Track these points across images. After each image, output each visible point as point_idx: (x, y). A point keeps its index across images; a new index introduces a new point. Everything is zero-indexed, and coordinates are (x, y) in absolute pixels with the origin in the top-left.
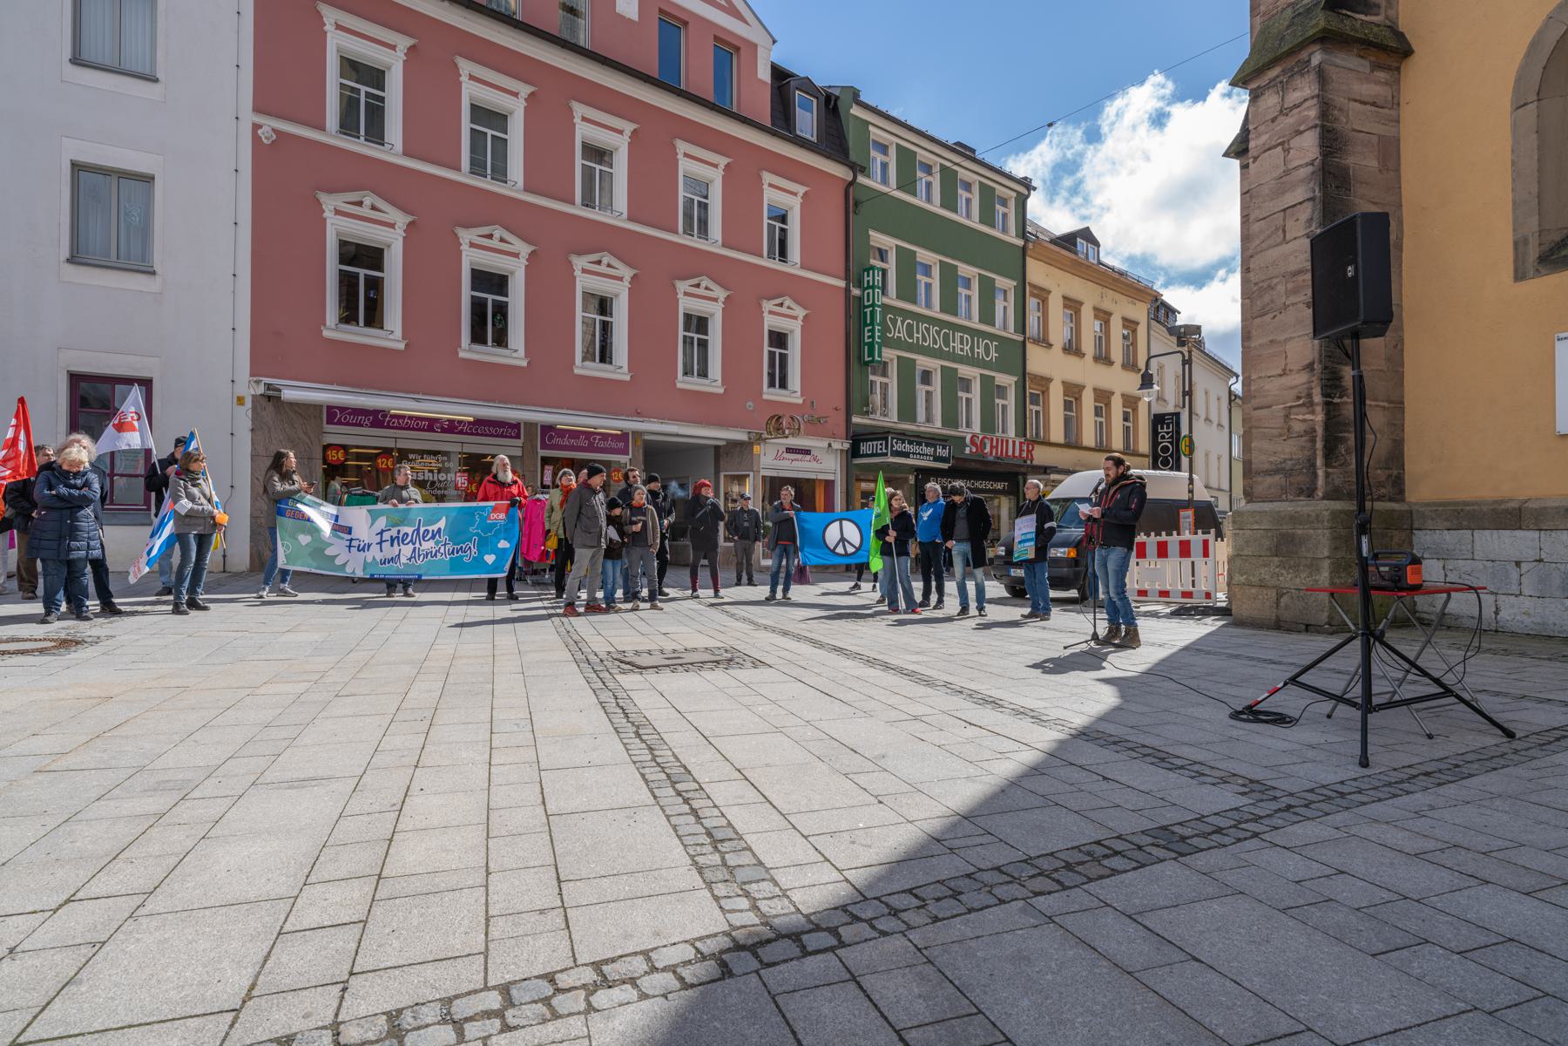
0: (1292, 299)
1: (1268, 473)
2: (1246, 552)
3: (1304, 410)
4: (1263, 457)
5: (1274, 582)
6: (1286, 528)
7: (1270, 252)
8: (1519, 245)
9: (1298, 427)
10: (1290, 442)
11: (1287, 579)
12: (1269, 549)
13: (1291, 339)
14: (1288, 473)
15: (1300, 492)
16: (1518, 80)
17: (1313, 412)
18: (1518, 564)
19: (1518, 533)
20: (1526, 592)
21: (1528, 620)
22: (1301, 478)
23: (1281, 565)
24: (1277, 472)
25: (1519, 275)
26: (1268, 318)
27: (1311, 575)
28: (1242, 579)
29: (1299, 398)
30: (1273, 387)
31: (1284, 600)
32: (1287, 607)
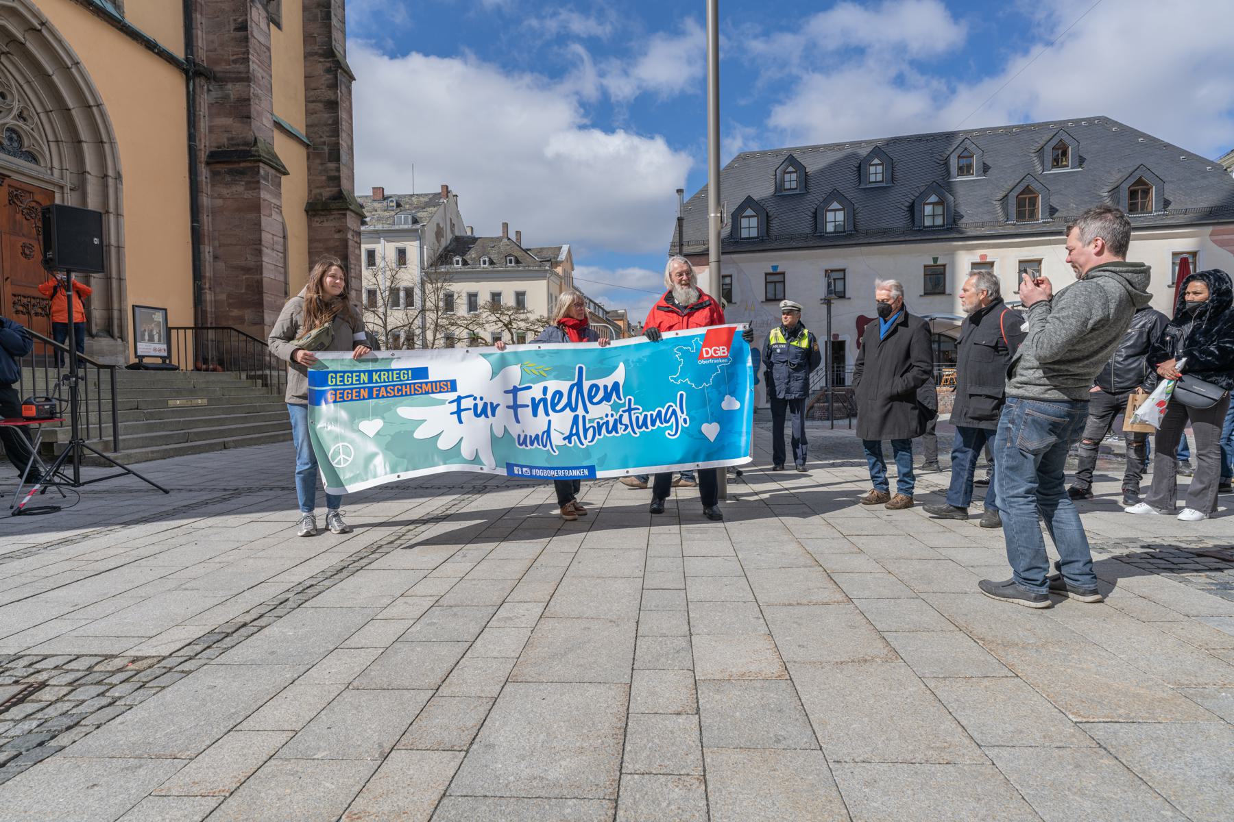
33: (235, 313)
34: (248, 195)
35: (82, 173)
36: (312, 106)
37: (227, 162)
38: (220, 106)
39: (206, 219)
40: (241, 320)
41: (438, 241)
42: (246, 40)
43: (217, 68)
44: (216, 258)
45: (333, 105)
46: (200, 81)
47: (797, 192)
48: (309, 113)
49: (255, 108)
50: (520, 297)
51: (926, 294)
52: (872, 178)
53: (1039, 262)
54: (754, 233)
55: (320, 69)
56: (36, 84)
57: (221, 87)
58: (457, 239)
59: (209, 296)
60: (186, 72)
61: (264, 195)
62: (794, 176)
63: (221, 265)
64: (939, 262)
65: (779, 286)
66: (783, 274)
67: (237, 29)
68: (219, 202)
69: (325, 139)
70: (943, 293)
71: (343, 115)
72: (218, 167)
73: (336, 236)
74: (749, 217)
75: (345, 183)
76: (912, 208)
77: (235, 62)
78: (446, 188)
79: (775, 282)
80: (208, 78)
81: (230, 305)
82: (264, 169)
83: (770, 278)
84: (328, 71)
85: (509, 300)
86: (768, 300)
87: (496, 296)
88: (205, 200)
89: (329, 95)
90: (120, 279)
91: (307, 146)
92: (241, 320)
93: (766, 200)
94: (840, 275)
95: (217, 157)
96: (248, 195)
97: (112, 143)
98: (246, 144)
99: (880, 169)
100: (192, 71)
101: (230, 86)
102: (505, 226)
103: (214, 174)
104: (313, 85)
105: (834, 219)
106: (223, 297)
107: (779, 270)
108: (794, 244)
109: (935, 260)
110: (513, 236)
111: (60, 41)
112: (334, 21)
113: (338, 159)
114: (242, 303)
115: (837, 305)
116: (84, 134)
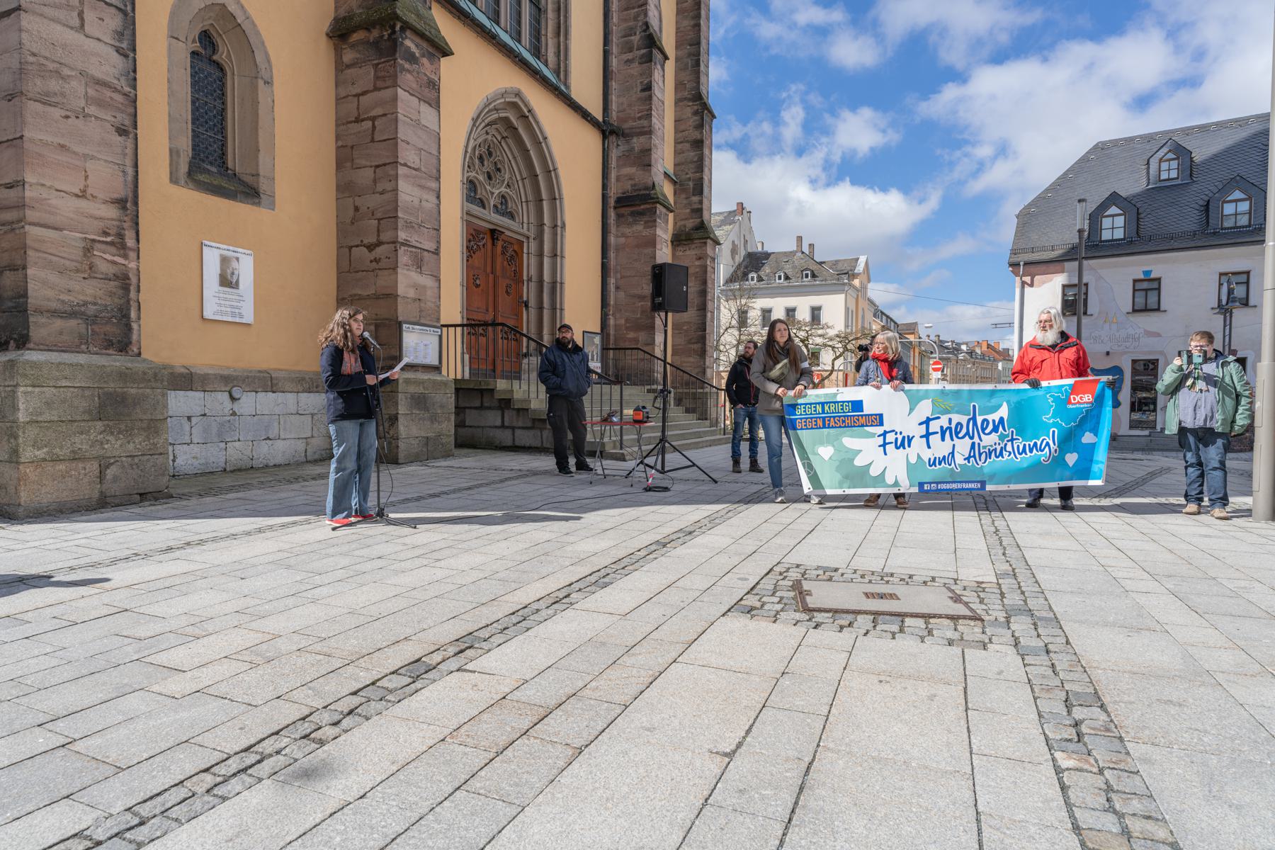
0: (92, 110)
1: (55, 313)
2: (46, 417)
3: (113, 250)
4: (50, 293)
5: (96, 451)
6: (112, 386)
7: (59, 28)
8: (174, 153)
9: (103, 267)
10: (94, 282)
11: (114, 446)
12: (90, 412)
13: (93, 158)
14: (91, 320)
15: (109, 344)
16: (173, 15)
17: (125, 257)
18: (189, 418)
19: (190, 393)
20: (195, 441)
21: (196, 463)
22: (108, 328)
23: (108, 430)
24: (72, 314)
25: (174, 180)
26: (57, 113)
27: (148, 438)
28: (40, 454)
29: (106, 234)
30: (67, 207)
31: (110, 473)
32: (115, 479)
33: (631, 335)
34: (646, 233)
35: (542, 225)
36: (680, 146)
37: (629, 205)
38: (626, 158)
39: (612, 255)
40: (636, 340)
42: (650, 98)
43: (625, 126)
44: (617, 288)
45: (698, 144)
46: (613, 138)
47: (1179, 182)
48: (676, 153)
49: (654, 156)
50: (816, 312)
54: (1119, 234)
55: (688, 111)
56: (519, 159)
57: (628, 142)
58: (750, 256)
59: (612, 322)
60: (603, 132)
61: (659, 232)
62: (1174, 164)
63: (622, 294)
65: (1156, 292)
66: (1159, 280)
67: (643, 90)
68: (622, 240)
69: (690, 175)
71: (706, 151)
72: (623, 210)
73: (697, 263)
74: (1113, 216)
75: (705, 213)
77: (640, 118)
78: (741, 205)
79: (1146, 290)
80: (617, 135)
81: (627, 328)
82: (660, 209)
83: (1139, 286)
84: (695, 113)
85: (803, 315)
86: (1134, 311)
87: (791, 311)
88: (612, 240)
89: (696, 135)
90: (562, 309)
91: (675, 183)
92: (636, 340)
93: (1138, 195)
94: (1243, 278)
95: (622, 202)
96: (646, 233)
97: (561, 199)
98: (646, 188)
100: (607, 131)
101: (635, 140)
102: (800, 239)
103: (619, 216)
104: (682, 127)
106: (623, 322)
107: (1152, 276)
108: (1176, 245)
110: (806, 249)
111: (537, 123)
112: (702, 68)
113: (701, 193)
114: (638, 327)
116: (544, 195)
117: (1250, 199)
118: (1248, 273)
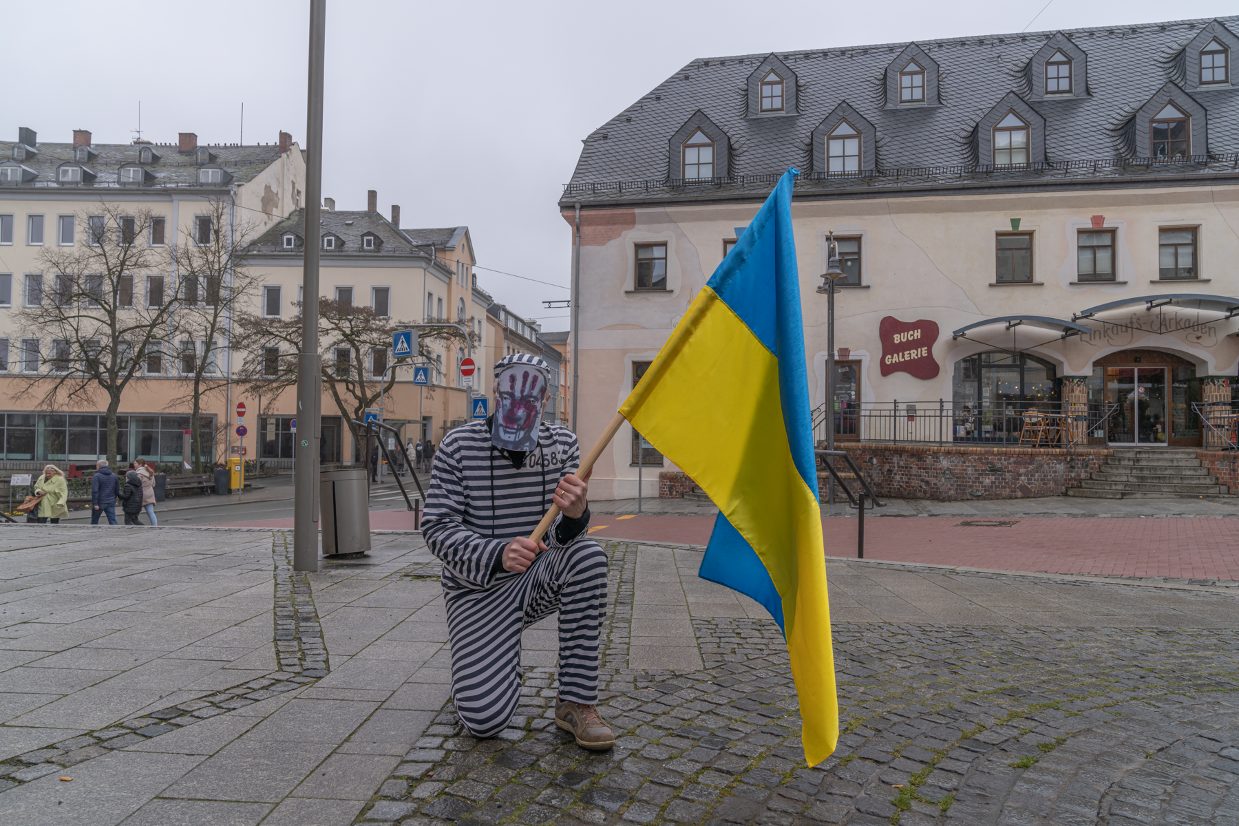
41: (266, 211)
47: (783, 114)
50: (382, 295)
51: (1001, 281)
52: (906, 95)
53: (1194, 230)
64: (1021, 228)
70: (1028, 280)
76: (973, 141)
85: (363, 299)
99: (918, 80)
102: (372, 195)
105: (844, 156)
109: (1015, 222)
110: (385, 211)
115: (844, 298)
117: (858, 135)
118: (858, 239)
